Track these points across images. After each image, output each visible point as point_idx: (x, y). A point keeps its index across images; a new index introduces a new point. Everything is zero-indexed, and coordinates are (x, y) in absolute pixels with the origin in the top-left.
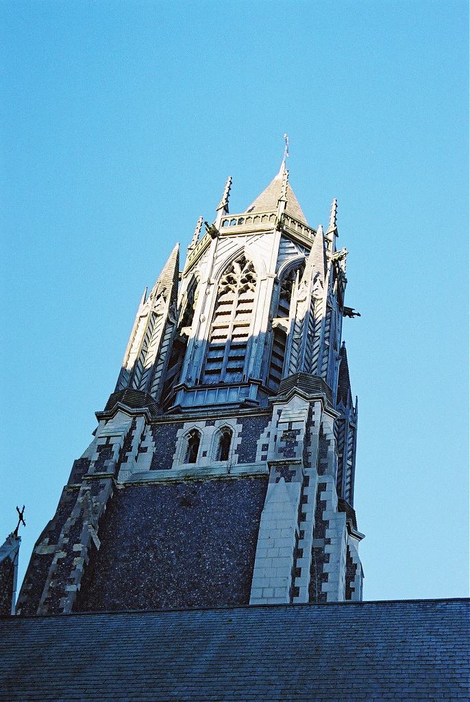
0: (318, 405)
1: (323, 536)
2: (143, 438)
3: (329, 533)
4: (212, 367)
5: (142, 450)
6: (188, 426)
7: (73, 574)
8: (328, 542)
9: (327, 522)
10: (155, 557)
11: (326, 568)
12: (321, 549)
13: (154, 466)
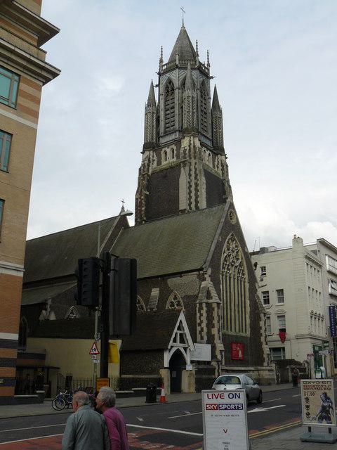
2: (153, 157)
3: (198, 177)
5: (153, 160)
6: (163, 150)
11: (199, 188)
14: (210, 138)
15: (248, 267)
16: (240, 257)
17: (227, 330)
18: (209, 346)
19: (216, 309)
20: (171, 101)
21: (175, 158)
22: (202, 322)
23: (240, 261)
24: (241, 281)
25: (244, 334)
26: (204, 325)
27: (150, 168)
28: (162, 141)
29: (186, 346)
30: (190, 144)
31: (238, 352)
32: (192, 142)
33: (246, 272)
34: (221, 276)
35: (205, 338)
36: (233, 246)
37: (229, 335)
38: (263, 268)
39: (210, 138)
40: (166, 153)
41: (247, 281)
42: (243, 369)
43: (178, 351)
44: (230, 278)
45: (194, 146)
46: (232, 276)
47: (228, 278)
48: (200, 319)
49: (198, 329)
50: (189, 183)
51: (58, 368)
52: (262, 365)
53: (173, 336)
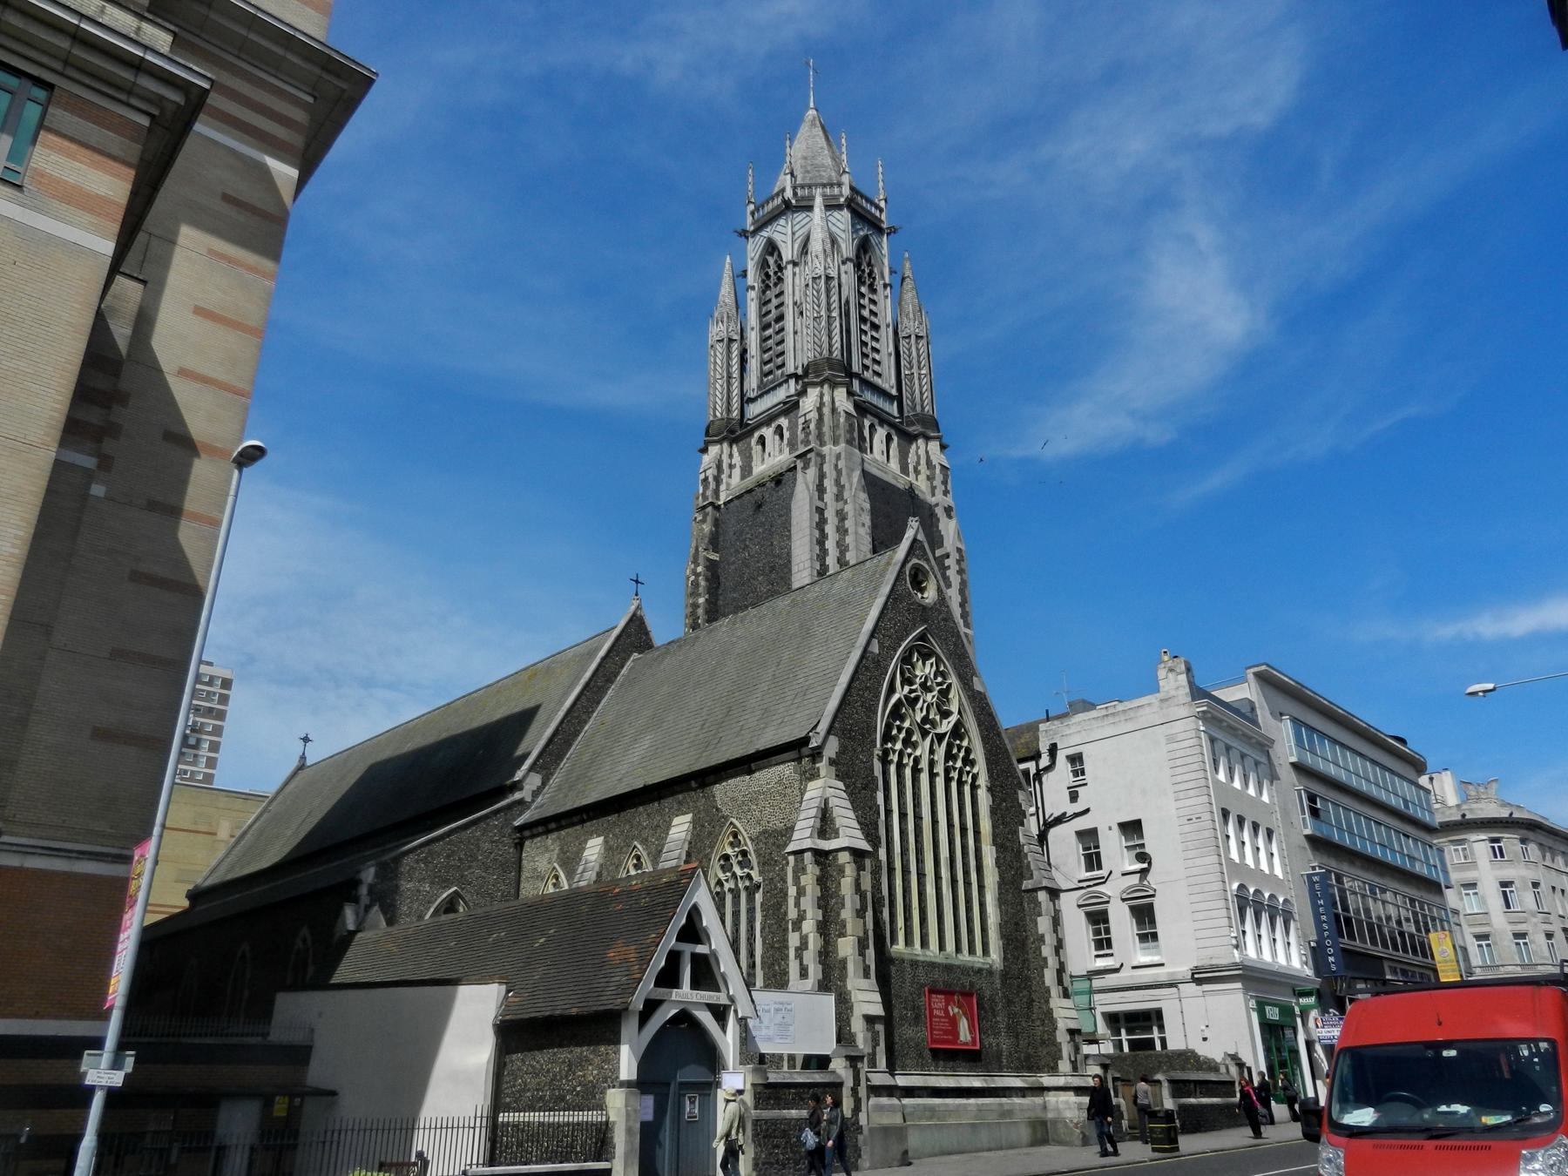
0: (826, 386)
1: (842, 499)
4: (767, 368)
5: (731, 466)
6: (757, 435)
7: (701, 590)
8: (846, 502)
9: (844, 485)
10: (749, 555)
12: (842, 510)
13: (743, 477)
14: (894, 392)
15: (985, 740)
16: (954, 708)
18: (830, 1000)
20: (775, 302)
21: (787, 450)
22: (802, 917)
23: (953, 719)
24: (960, 783)
25: (978, 960)
26: (809, 926)
27: (723, 487)
28: (754, 410)
29: (720, 998)
30: (822, 404)
31: (954, 1022)
32: (827, 398)
33: (979, 754)
34: (877, 766)
35: (815, 971)
36: (924, 670)
37: (915, 964)
38: (1076, 759)
39: (894, 392)
40: (762, 441)
41: (983, 781)
42: (977, 1083)
43: (684, 1018)
44: (916, 771)
45: (834, 410)
46: (924, 764)
47: (908, 772)
48: (797, 904)
49: (794, 940)
50: (820, 511)
51: (333, 1093)
52: (1053, 1069)
53: (659, 962)
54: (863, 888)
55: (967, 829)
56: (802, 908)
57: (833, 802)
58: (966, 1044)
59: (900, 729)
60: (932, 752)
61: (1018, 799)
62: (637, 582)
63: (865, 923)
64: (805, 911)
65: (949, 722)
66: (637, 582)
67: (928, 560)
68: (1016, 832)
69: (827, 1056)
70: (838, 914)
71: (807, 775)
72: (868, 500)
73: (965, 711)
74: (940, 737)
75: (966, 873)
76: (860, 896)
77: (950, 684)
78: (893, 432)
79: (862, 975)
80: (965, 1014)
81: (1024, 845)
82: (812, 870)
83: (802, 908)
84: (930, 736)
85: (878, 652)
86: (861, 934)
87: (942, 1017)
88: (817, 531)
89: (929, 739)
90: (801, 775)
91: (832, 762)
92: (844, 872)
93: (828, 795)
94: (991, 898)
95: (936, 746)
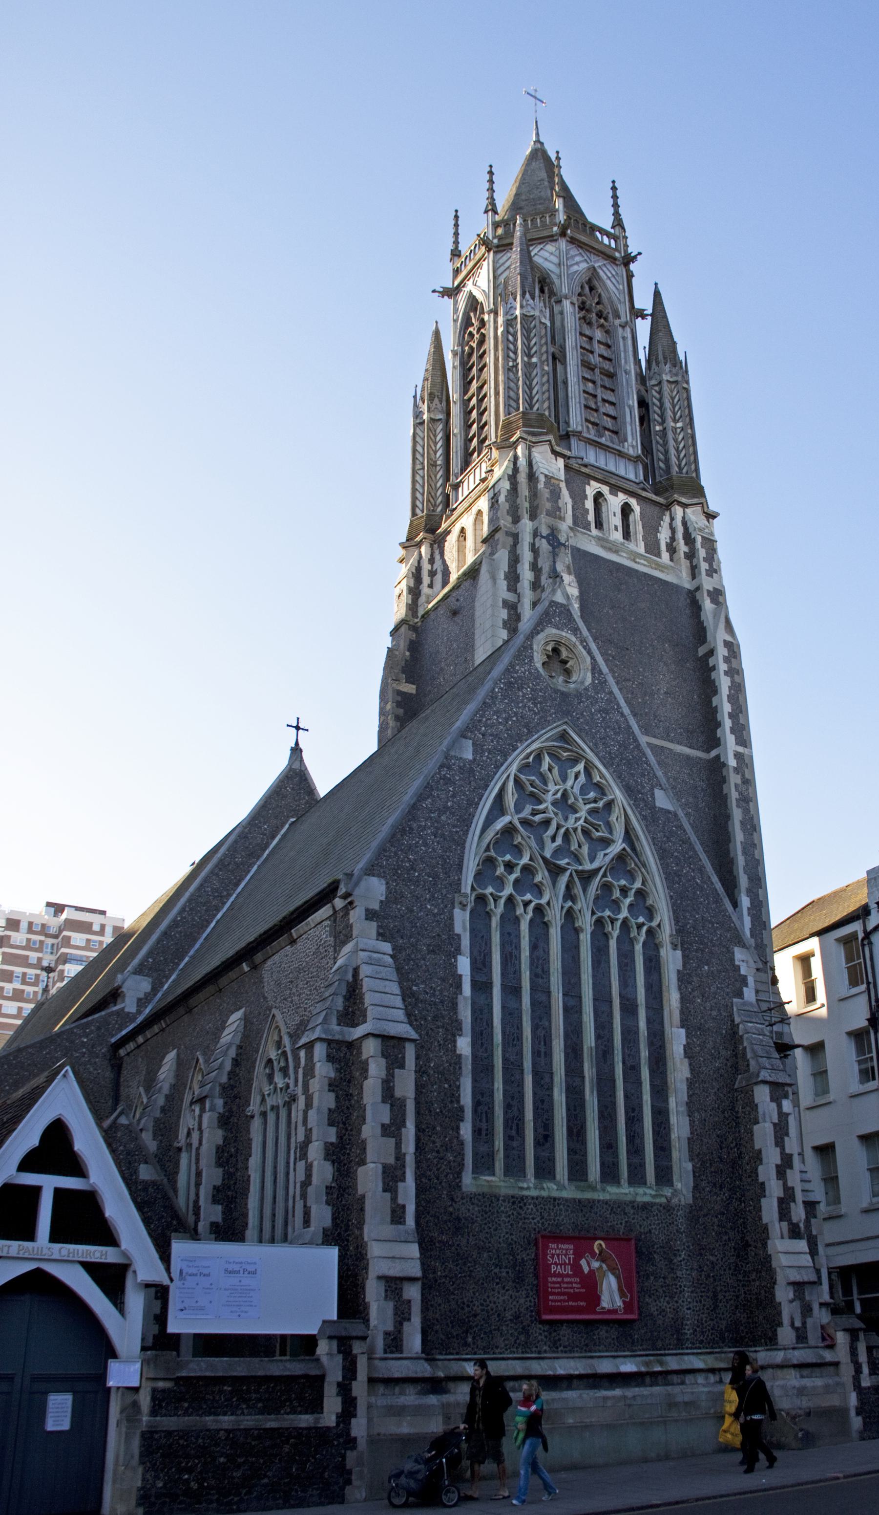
8: (543, 590)
17: (515, 1168)
18: (333, 1253)
19: (376, 1069)
23: (618, 846)
34: (461, 920)
37: (518, 1201)
41: (666, 934)
45: (532, 476)
46: (555, 917)
54: (398, 1093)
55: (637, 1006)
56: (309, 1127)
57: (365, 970)
58: (614, 1311)
59: (510, 867)
60: (569, 895)
61: (732, 960)
62: (298, 728)
63: (398, 1145)
64: (311, 1129)
65: (605, 855)
66: (298, 728)
67: (576, 630)
68: (729, 1007)
69: (314, 1336)
70: (359, 1131)
71: (342, 937)
72: (575, 584)
73: (638, 839)
74: (586, 877)
75: (632, 1070)
76: (392, 1105)
77: (613, 801)
78: (633, 502)
79: (389, 1219)
80: (612, 1270)
81: (738, 1025)
82: (323, 1070)
83: (309, 1127)
84: (568, 873)
85: (470, 757)
86: (391, 1160)
87: (568, 1276)
88: (506, 631)
89: (564, 880)
90: (335, 937)
91: (370, 915)
92: (367, 1070)
93: (359, 962)
94: (677, 1102)
95: (578, 889)
